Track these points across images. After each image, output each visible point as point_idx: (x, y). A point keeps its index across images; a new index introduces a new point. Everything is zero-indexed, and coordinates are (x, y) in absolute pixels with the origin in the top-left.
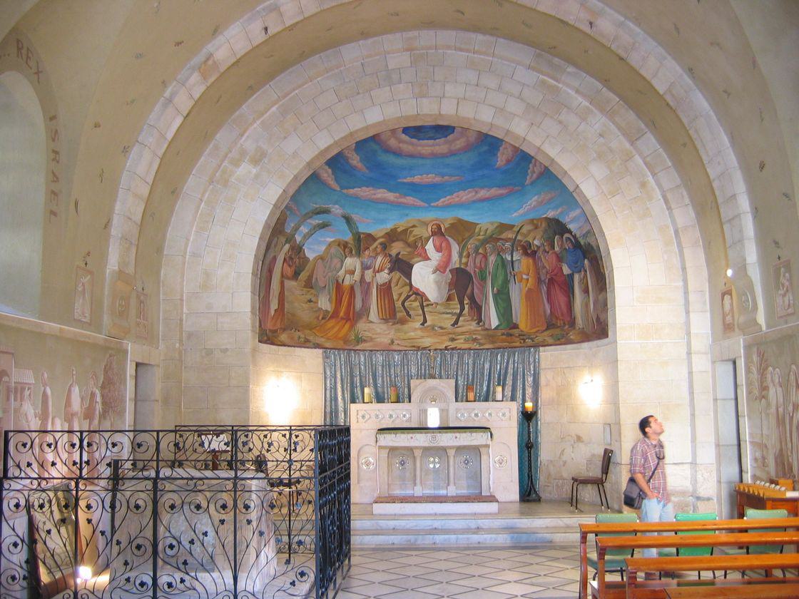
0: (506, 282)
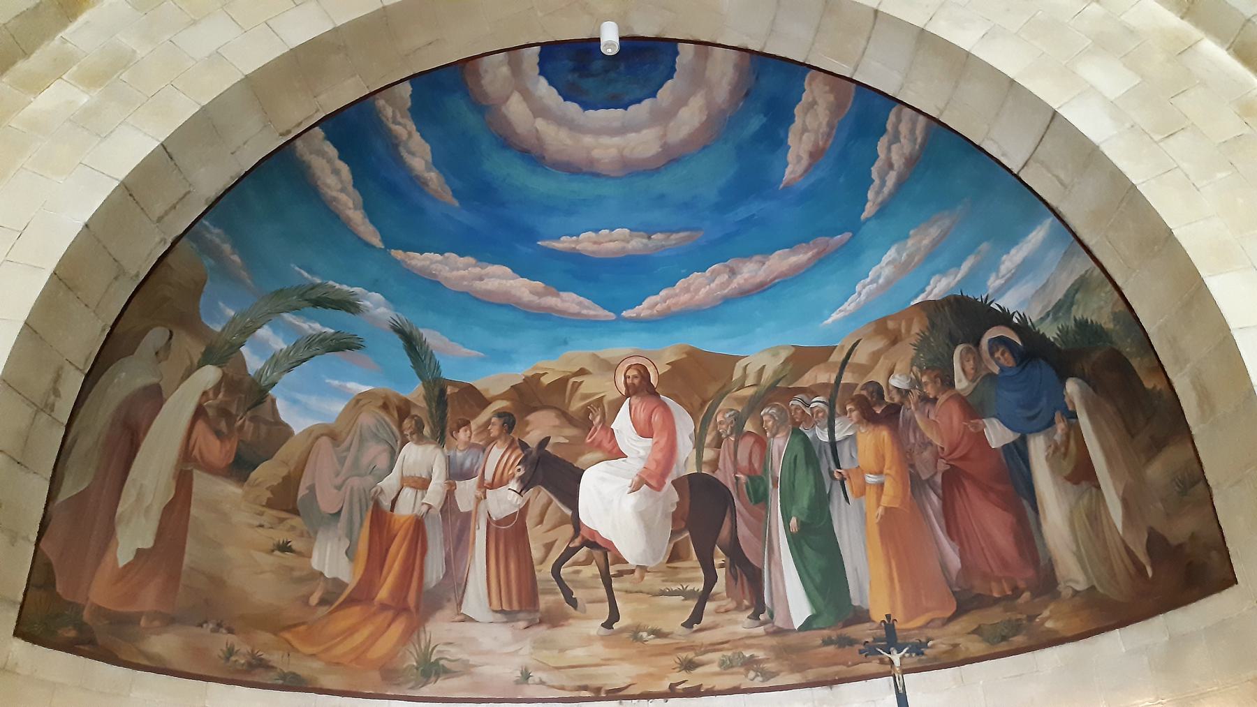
0: (821, 502)
